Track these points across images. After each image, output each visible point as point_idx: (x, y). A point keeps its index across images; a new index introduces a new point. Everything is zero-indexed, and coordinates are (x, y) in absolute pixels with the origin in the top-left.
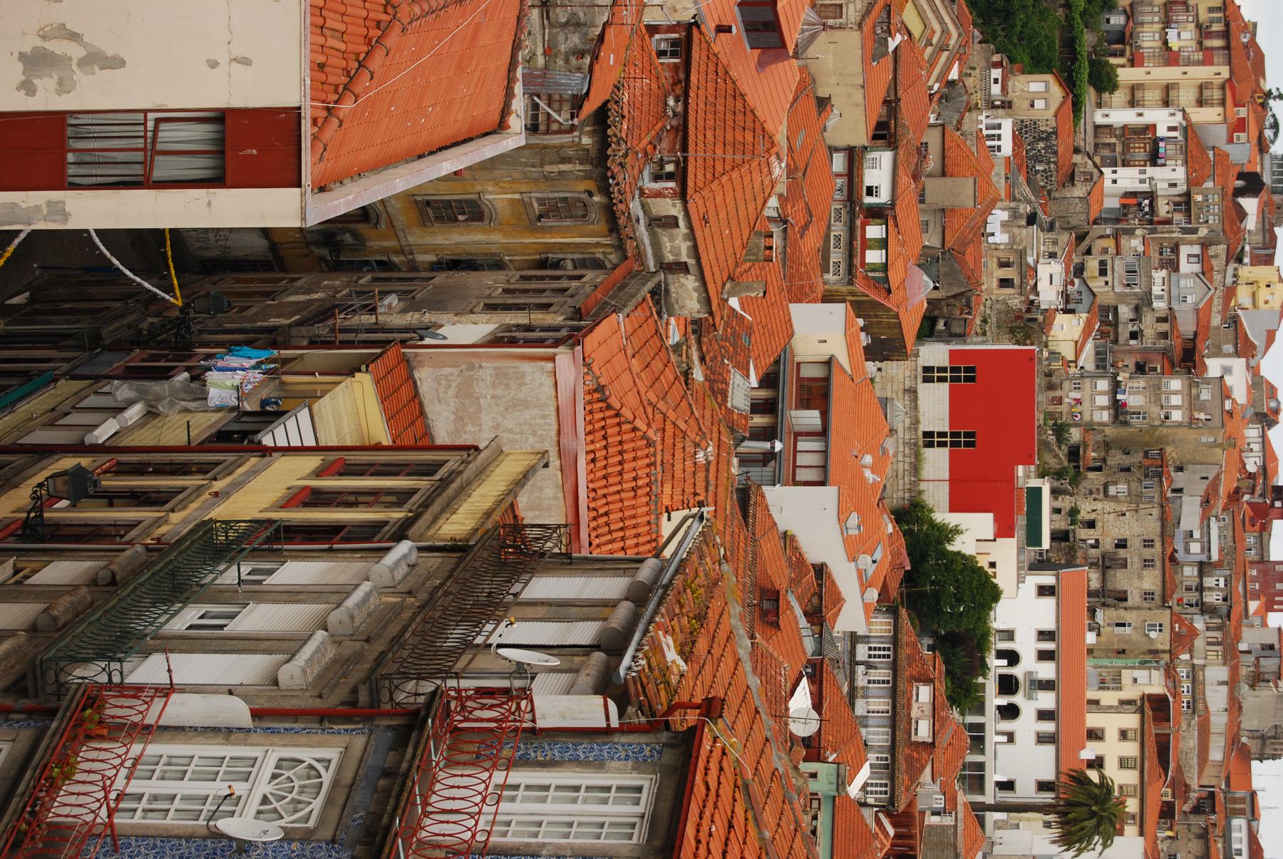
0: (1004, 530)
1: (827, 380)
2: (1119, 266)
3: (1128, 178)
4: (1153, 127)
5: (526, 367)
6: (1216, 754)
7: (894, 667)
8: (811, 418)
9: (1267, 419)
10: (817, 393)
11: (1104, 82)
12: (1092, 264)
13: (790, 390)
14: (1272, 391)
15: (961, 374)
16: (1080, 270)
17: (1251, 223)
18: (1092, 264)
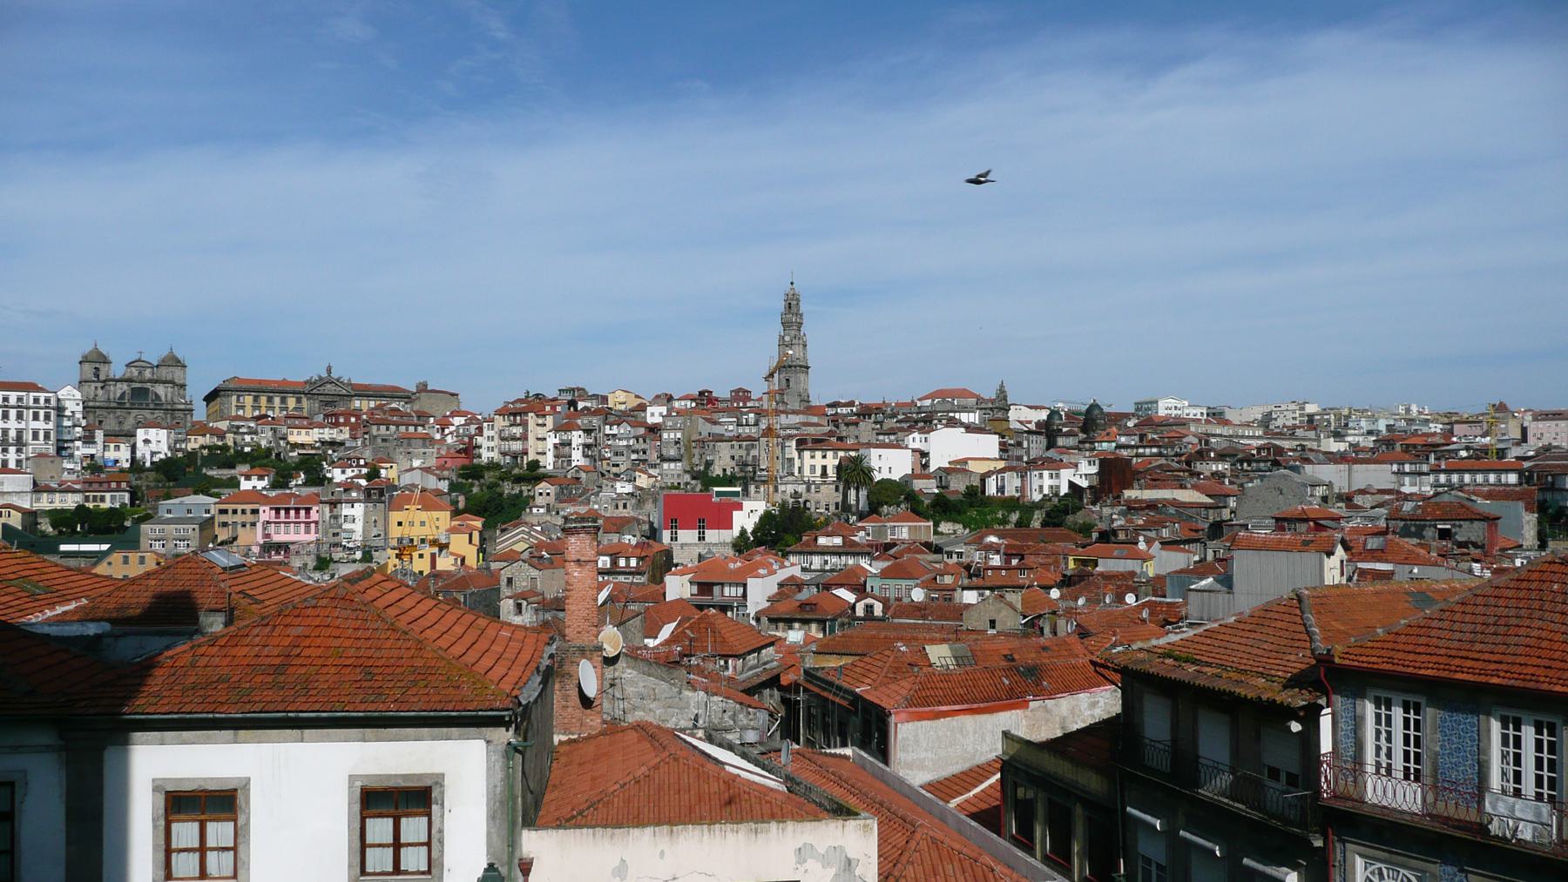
0: (739, 507)
1: (699, 584)
2: (616, 459)
3: (578, 458)
4: (555, 446)
5: (899, 736)
6: (815, 419)
7: (811, 553)
8: (716, 589)
9: (670, 399)
10: (705, 588)
11: (534, 465)
12: (615, 470)
13: (706, 599)
14: (658, 397)
15: (674, 524)
16: (617, 475)
17: (588, 404)
18: (615, 470)
